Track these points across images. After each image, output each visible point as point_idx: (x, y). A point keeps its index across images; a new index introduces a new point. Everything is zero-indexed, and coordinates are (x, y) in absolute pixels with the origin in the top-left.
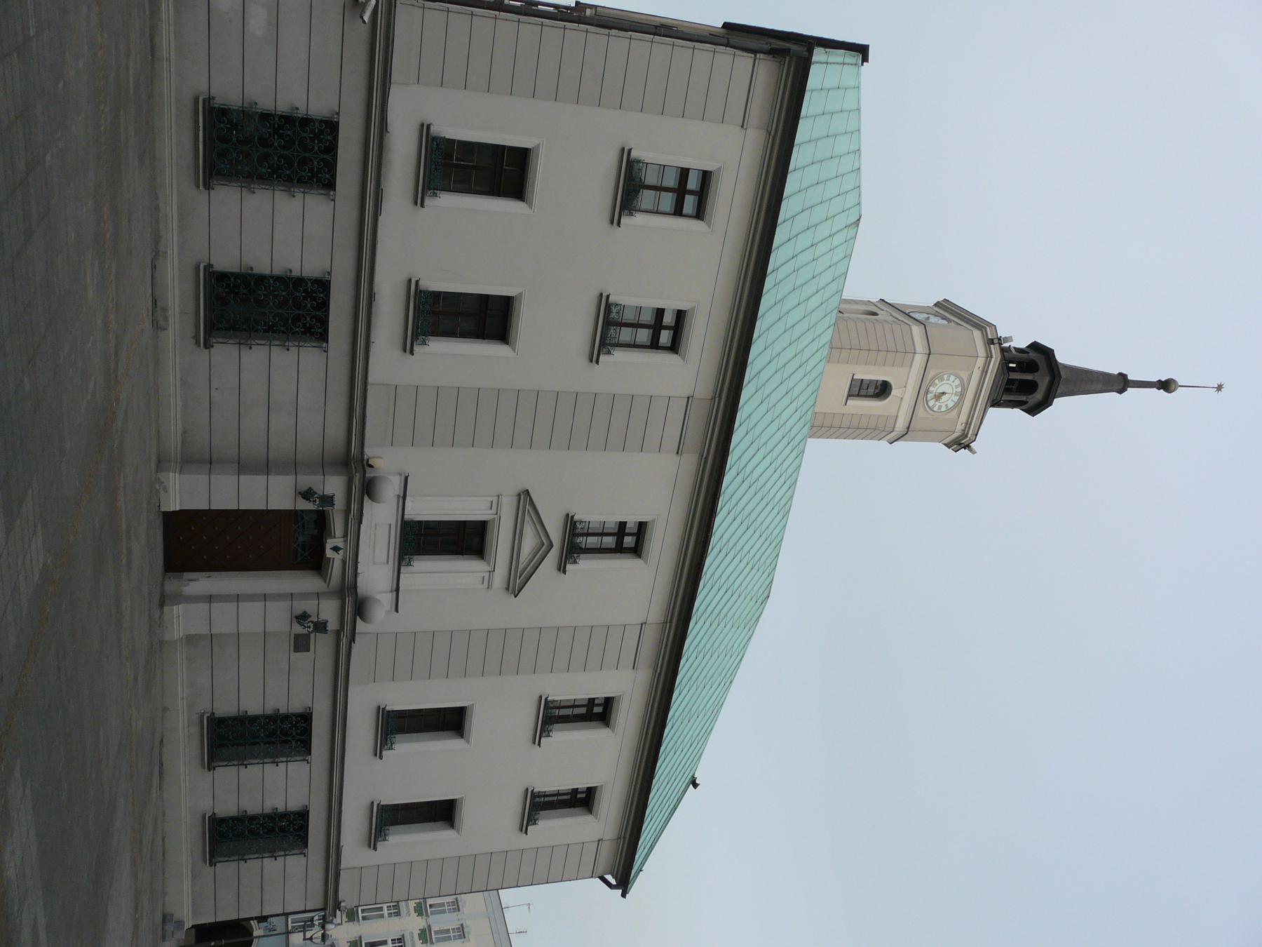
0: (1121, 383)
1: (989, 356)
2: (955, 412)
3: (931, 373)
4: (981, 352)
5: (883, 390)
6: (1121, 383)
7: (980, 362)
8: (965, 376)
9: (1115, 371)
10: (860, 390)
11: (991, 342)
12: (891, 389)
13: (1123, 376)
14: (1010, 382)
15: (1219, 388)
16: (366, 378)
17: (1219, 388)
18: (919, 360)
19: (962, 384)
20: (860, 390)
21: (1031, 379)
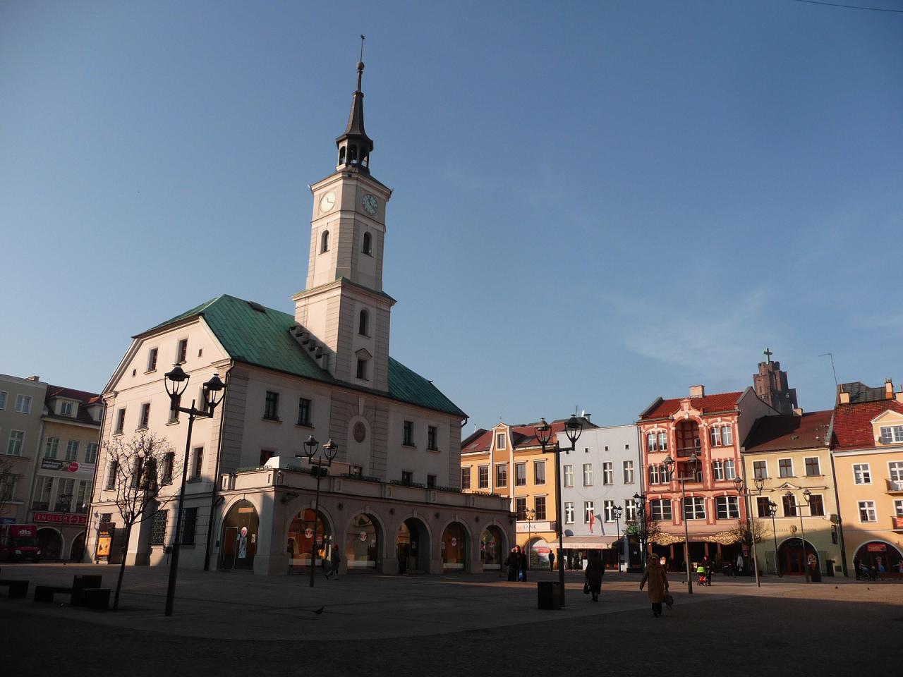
0: (359, 96)
1: (357, 179)
3: (362, 211)
5: (367, 237)
6: (359, 96)
7: (359, 184)
10: (366, 250)
11: (350, 176)
12: (369, 234)
15: (363, 37)
16: (378, 498)
17: (363, 37)
18: (358, 218)
20: (366, 250)
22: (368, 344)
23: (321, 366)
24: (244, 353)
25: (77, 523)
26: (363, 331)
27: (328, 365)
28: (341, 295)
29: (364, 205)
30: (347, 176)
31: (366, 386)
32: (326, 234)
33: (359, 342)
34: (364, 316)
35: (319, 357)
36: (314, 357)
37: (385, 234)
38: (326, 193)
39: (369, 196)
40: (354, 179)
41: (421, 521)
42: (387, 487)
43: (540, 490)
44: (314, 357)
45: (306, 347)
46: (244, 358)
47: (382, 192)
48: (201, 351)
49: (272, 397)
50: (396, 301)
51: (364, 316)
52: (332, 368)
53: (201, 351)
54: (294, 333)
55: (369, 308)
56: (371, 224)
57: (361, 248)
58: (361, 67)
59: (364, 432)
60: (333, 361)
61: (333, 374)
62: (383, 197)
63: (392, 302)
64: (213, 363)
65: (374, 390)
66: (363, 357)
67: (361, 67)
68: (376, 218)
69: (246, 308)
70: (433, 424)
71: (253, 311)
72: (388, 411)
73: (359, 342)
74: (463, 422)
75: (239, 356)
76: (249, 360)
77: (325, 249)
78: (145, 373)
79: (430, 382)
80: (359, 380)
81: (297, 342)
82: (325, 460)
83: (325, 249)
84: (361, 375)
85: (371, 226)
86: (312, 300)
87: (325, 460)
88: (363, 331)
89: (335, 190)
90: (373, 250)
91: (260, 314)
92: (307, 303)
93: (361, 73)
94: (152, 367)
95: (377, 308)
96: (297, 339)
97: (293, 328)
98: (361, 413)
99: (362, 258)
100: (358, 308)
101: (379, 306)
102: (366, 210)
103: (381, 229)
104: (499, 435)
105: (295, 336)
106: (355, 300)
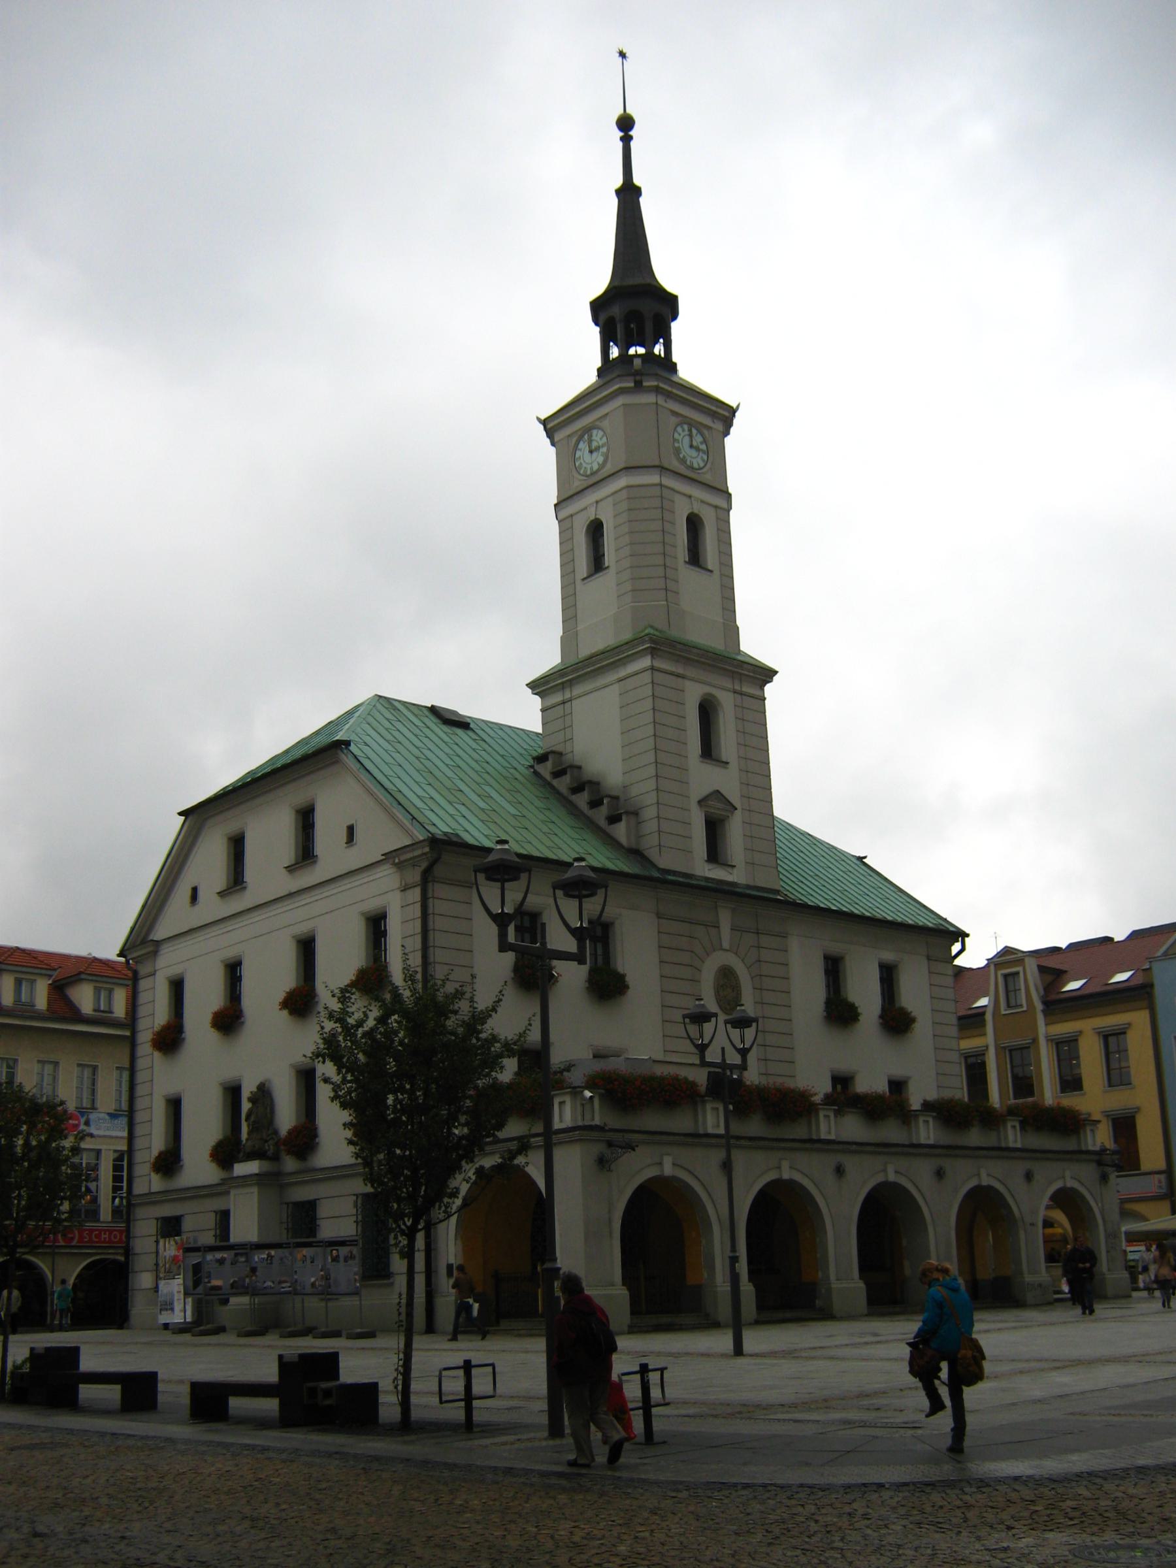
0: (629, 194)
1: (657, 390)
2: (706, 432)
3: (675, 465)
4: (650, 398)
5: (694, 524)
6: (629, 194)
8: (674, 420)
9: (614, 202)
10: (695, 558)
11: (638, 385)
13: (619, 192)
15: (622, 55)
17: (622, 55)
18: (669, 481)
19: (681, 424)
20: (695, 558)
22: (727, 782)
23: (623, 840)
24: (454, 825)
25: (74, 1243)
26: (708, 750)
27: (639, 837)
28: (652, 668)
29: (677, 451)
30: (632, 385)
31: (730, 878)
32: (596, 530)
33: (704, 778)
34: (707, 711)
35: (614, 819)
36: (603, 823)
37: (731, 513)
38: (588, 430)
39: (686, 427)
40: (650, 390)
41: (904, 1188)
42: (821, 1114)
43: (1119, 1100)
44: (603, 823)
45: (582, 800)
46: (457, 835)
47: (714, 415)
48: (351, 830)
49: (527, 920)
50: (776, 672)
51: (707, 711)
52: (649, 844)
53: (351, 830)
54: (545, 770)
56: (697, 492)
57: (682, 553)
58: (626, 124)
59: (736, 988)
60: (650, 827)
61: (653, 855)
62: (719, 426)
63: (768, 674)
64: (388, 856)
65: (748, 887)
66: (716, 808)
67: (626, 124)
68: (707, 478)
69: (426, 720)
70: (888, 956)
71: (445, 728)
72: (784, 936)
73: (704, 778)
74: (956, 947)
75: (445, 834)
76: (471, 841)
77: (598, 564)
78: (222, 894)
79: (861, 859)
80: (711, 866)
81: (552, 787)
82: (734, 1058)
83: (598, 564)
84: (714, 854)
85: (695, 499)
86: (578, 690)
87: (734, 1058)
88: (708, 750)
89: (605, 424)
90: (710, 556)
91: (459, 731)
92: (568, 695)
93: (626, 140)
94: (237, 879)
96: (555, 782)
97: (542, 759)
98: (726, 945)
99: (688, 576)
100: (693, 694)
101: (737, 687)
102: (683, 461)
103: (719, 501)
104: (1006, 976)
105: (548, 777)
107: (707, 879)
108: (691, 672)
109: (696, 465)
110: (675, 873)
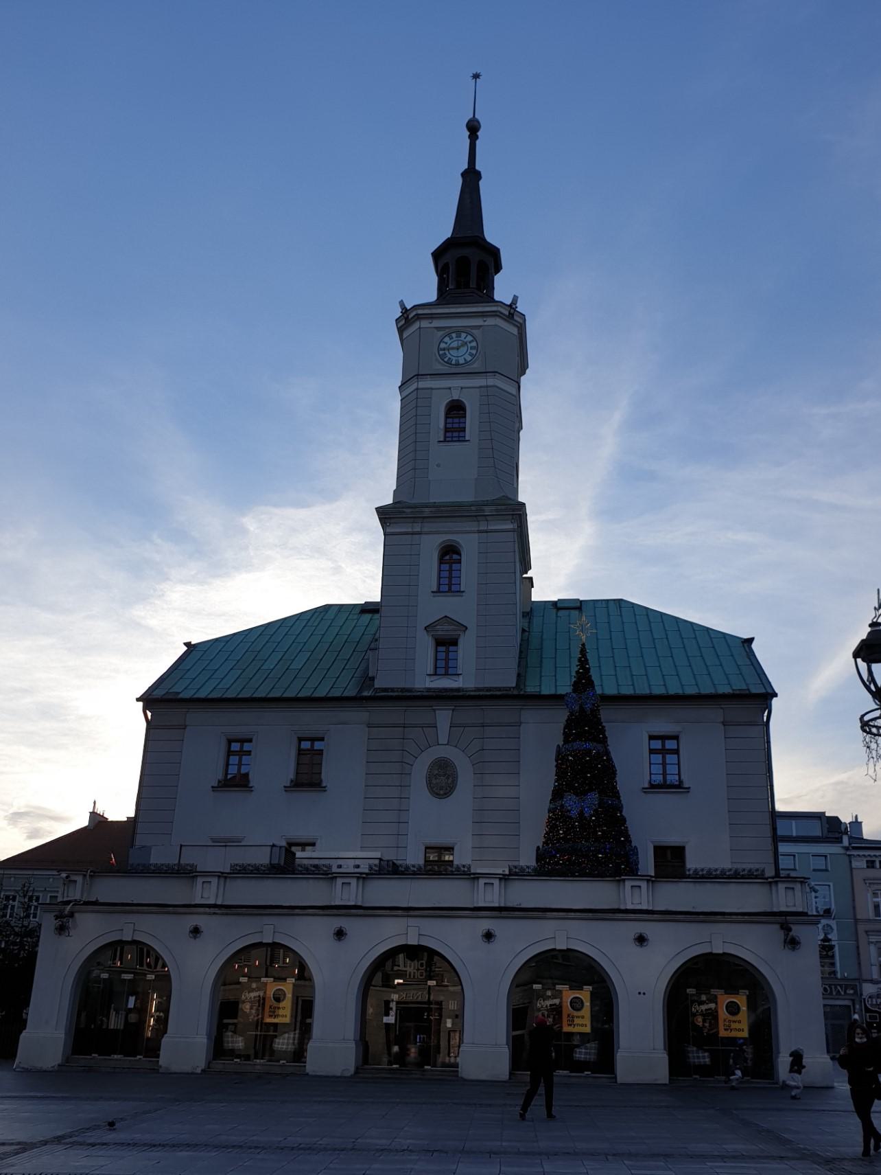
0: (471, 177)
4: (416, 326)
6: (471, 177)
9: (459, 182)
13: (463, 175)
14: (458, 286)
21: (467, 263)
34: (450, 553)
55: (459, 539)
58: (473, 128)
65: (478, 689)
66: (444, 631)
67: (473, 128)
73: (433, 608)
84: (444, 667)
95: (479, 532)
98: (443, 740)
102: (449, 363)
106: (419, 533)
107: (429, 690)
108: (428, 527)
109: (462, 361)
110: (392, 690)
